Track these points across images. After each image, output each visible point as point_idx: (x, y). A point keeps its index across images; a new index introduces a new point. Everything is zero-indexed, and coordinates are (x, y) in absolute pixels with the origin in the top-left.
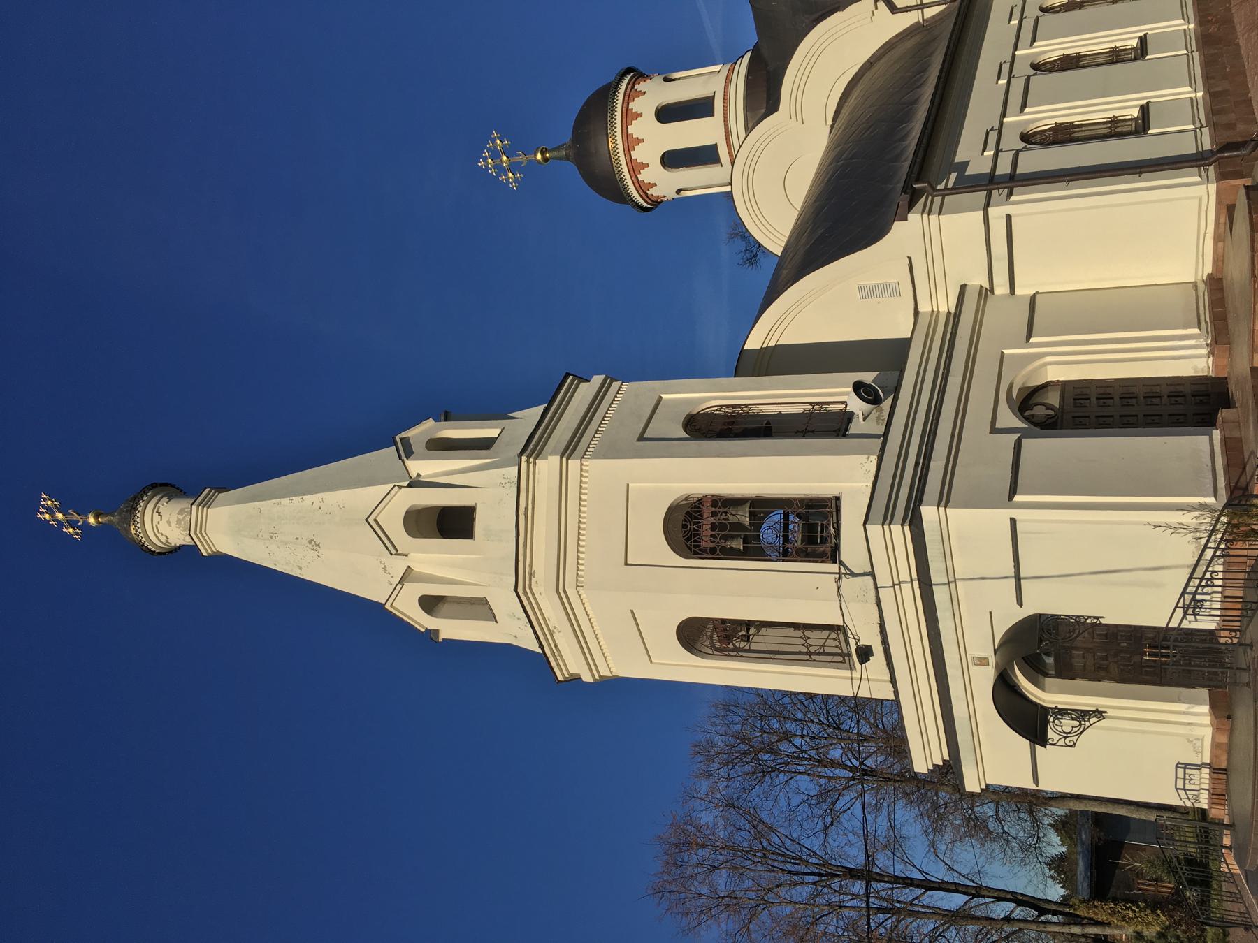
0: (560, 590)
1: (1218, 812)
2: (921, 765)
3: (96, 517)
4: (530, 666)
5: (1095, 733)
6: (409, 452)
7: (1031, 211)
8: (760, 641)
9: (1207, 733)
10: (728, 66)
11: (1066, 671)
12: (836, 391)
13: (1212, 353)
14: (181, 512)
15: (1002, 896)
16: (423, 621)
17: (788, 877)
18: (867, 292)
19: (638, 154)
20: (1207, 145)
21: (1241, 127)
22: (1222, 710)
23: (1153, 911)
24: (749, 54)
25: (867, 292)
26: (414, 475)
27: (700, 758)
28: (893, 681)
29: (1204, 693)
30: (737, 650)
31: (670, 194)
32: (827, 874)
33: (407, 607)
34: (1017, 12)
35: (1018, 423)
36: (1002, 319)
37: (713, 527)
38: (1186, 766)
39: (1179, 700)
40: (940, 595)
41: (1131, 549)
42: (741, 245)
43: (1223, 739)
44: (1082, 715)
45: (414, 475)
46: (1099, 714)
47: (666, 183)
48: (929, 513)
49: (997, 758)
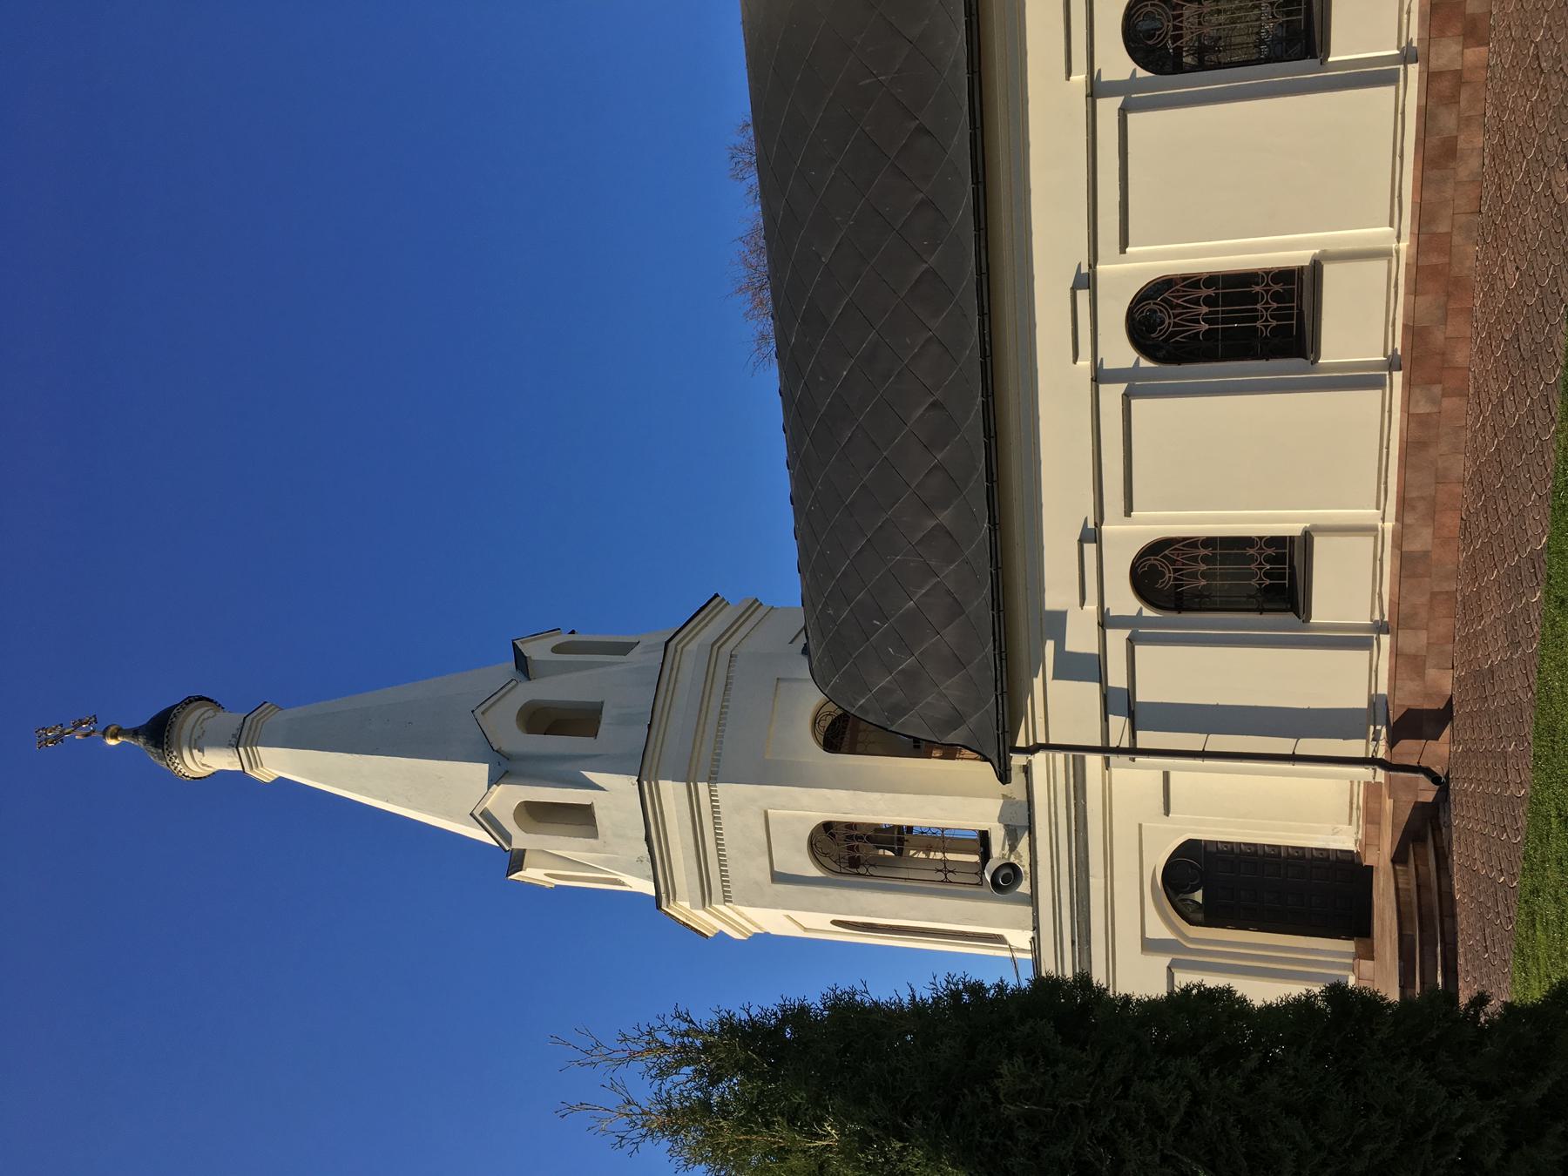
3: (114, 737)
20: (1383, 689)
21: (1431, 673)
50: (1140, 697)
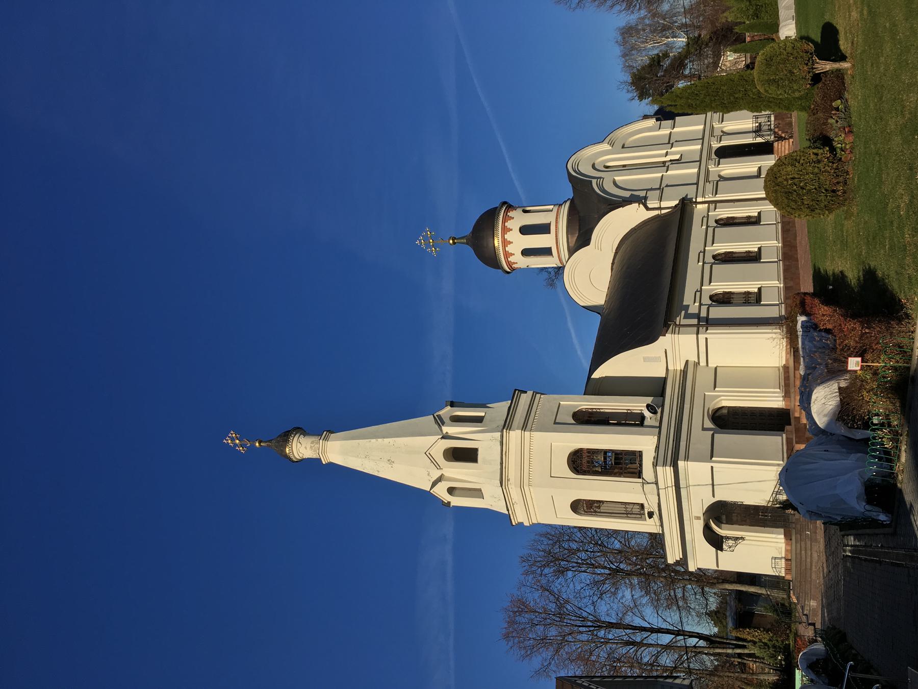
0: (521, 487)
1: (788, 577)
2: (671, 560)
4: (506, 518)
5: (741, 547)
6: (440, 422)
7: (717, 338)
8: (603, 509)
9: (783, 546)
10: (556, 209)
11: (730, 522)
12: (638, 405)
13: (784, 400)
14: (312, 443)
15: (692, 635)
16: (446, 497)
17: (576, 628)
18: (646, 359)
19: (509, 249)
20: (783, 313)
22: (788, 536)
23: (767, 632)
24: (568, 204)
25: (646, 359)
26: (444, 432)
27: (524, 564)
28: (662, 525)
29: (782, 530)
30: (595, 512)
31: (524, 266)
32: (599, 626)
33: (440, 491)
34: (705, 219)
35: (711, 426)
36: (704, 378)
37: (588, 462)
38: (775, 558)
39: (773, 533)
40: (683, 492)
41: (755, 478)
42: (545, 275)
43: (789, 548)
44: (736, 539)
45: (444, 432)
46: (742, 538)
47: (521, 262)
48: (681, 464)
49: (703, 558)
50: (710, 317)
